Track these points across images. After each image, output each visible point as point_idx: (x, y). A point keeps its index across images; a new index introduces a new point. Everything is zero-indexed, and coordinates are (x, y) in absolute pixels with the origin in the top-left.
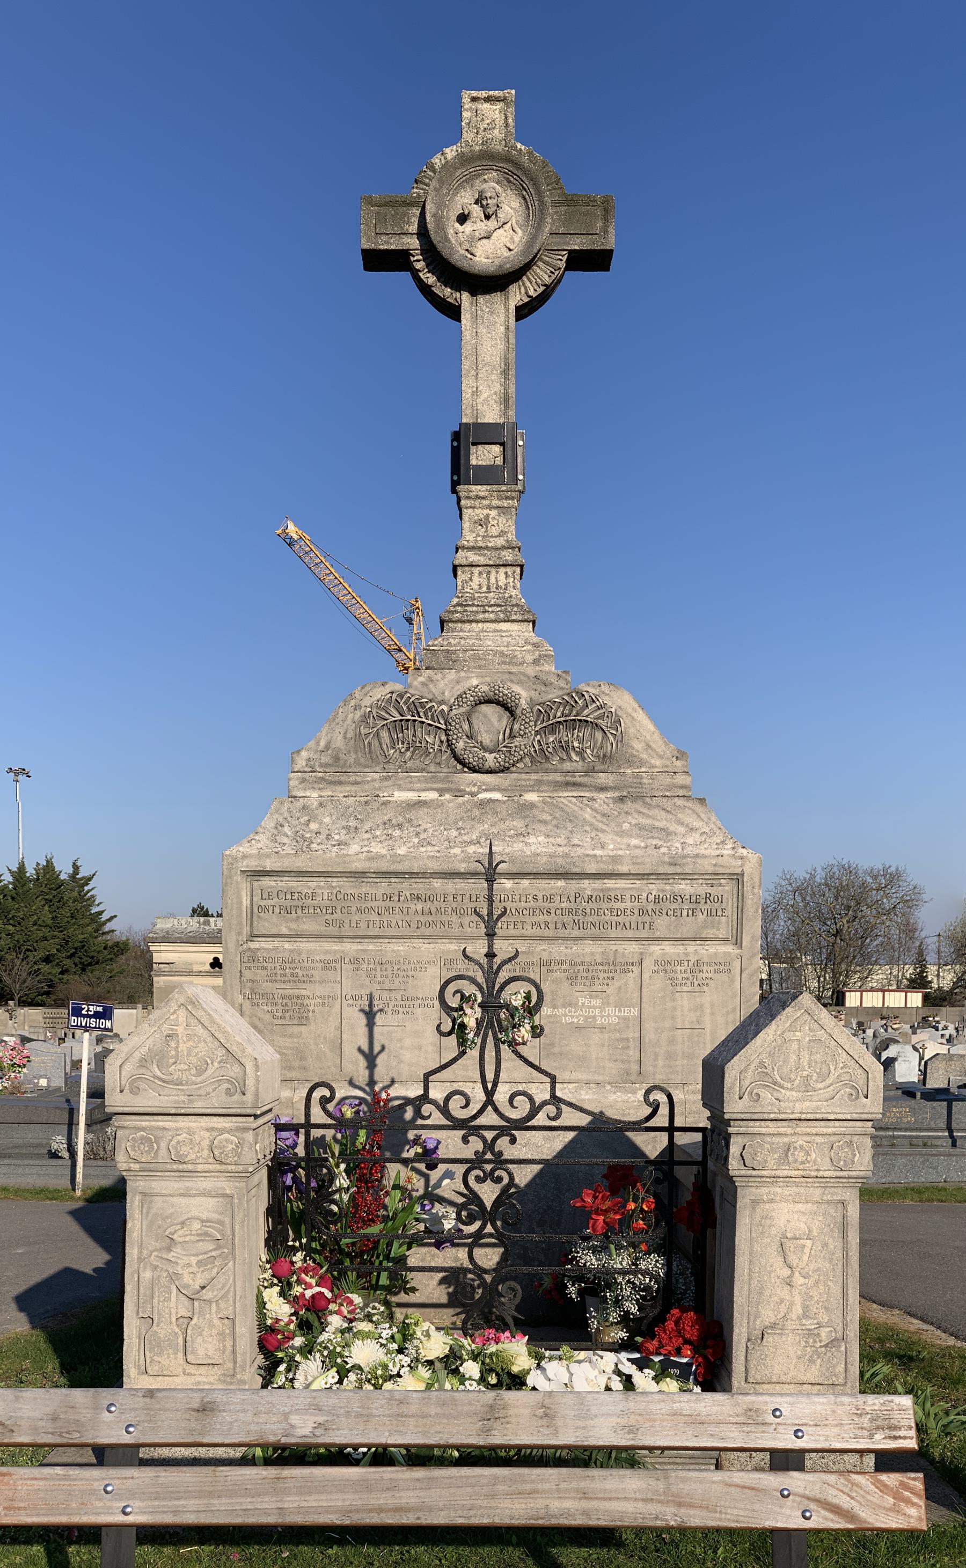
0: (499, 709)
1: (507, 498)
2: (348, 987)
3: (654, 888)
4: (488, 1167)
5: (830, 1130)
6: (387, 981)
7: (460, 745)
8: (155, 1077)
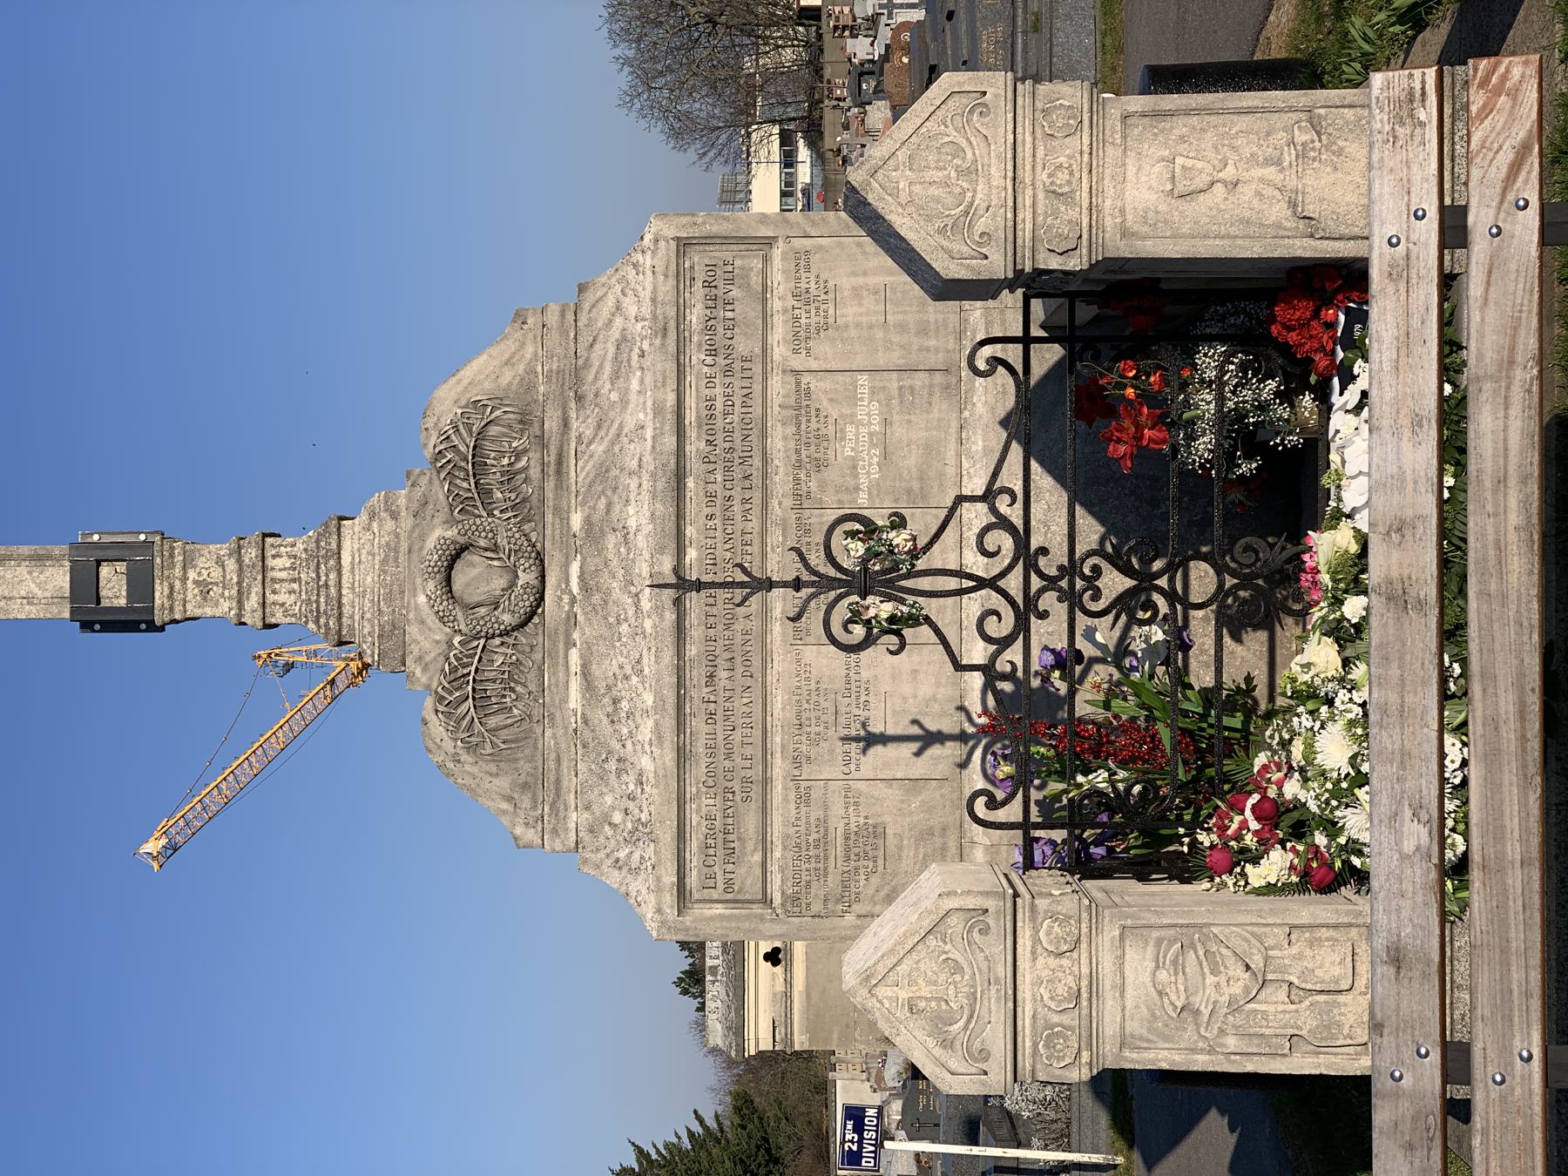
0: (458, 566)
1: (172, 556)
2: (833, 771)
3: (696, 356)
4: (1079, 584)
5: (1029, 139)
7: (507, 619)
8: (966, 1028)
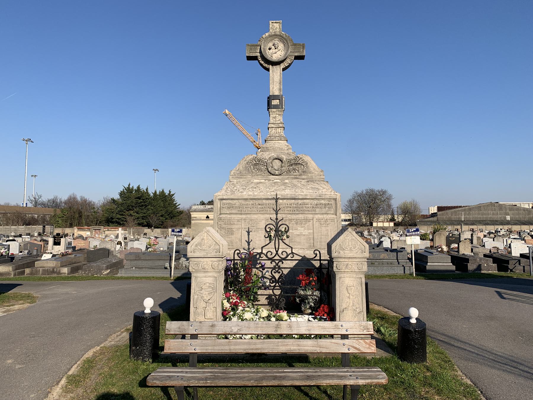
3: (316, 202)
4: (277, 269)
7: (270, 169)
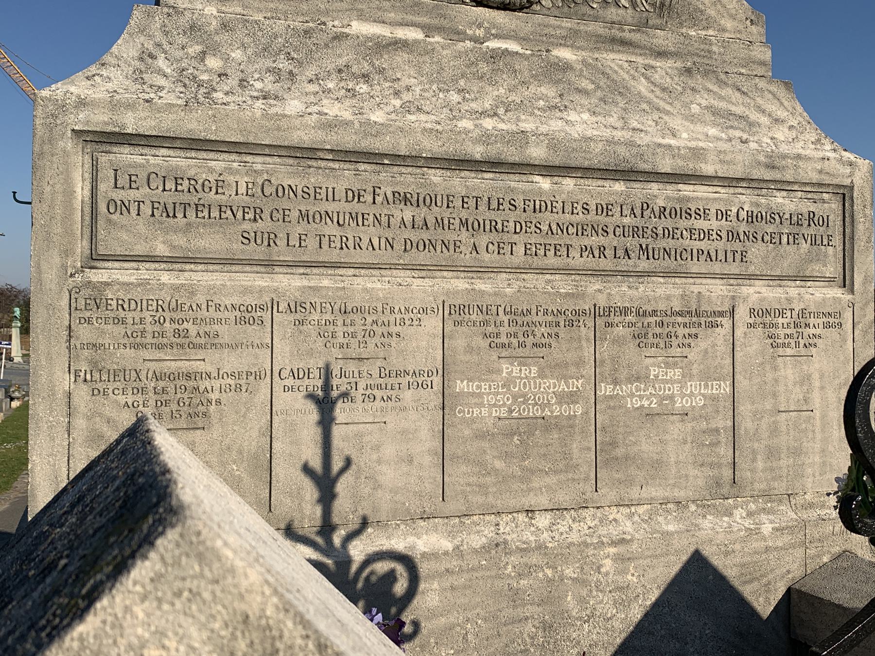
3: (746, 200)
6: (354, 343)
